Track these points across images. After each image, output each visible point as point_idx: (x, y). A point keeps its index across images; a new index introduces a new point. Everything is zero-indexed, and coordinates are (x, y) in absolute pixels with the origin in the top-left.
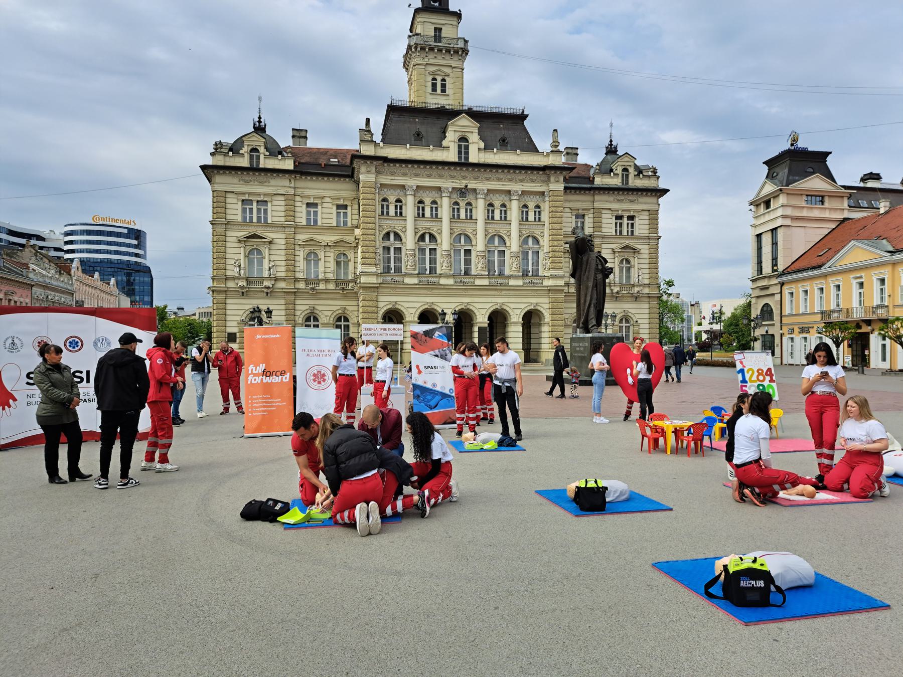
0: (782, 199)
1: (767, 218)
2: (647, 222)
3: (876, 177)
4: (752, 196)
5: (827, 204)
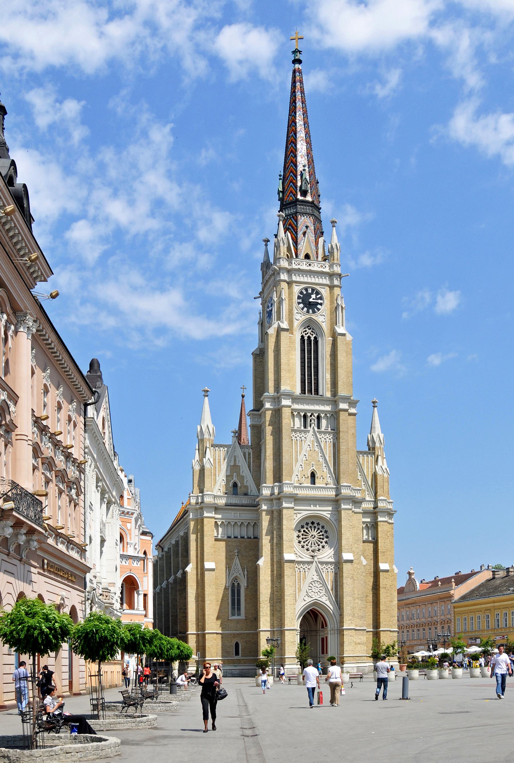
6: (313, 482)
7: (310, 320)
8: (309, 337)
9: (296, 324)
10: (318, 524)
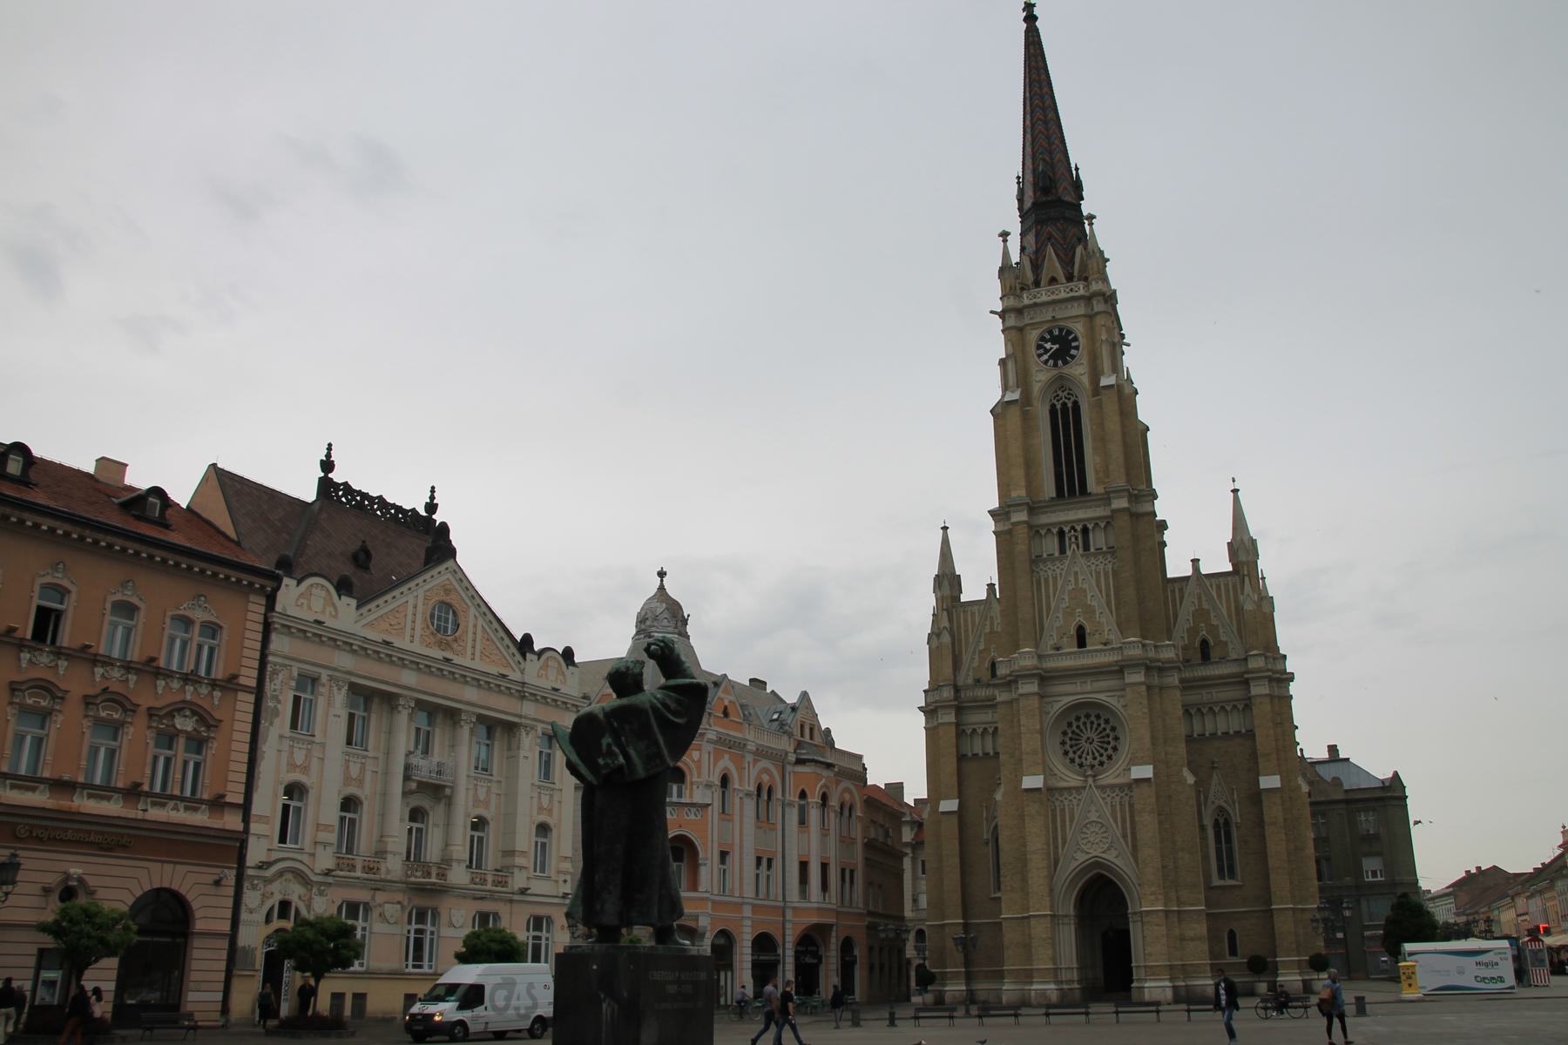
6: (1082, 642)
7: (1061, 377)
8: (1064, 404)
9: (1036, 388)
10: (1098, 717)
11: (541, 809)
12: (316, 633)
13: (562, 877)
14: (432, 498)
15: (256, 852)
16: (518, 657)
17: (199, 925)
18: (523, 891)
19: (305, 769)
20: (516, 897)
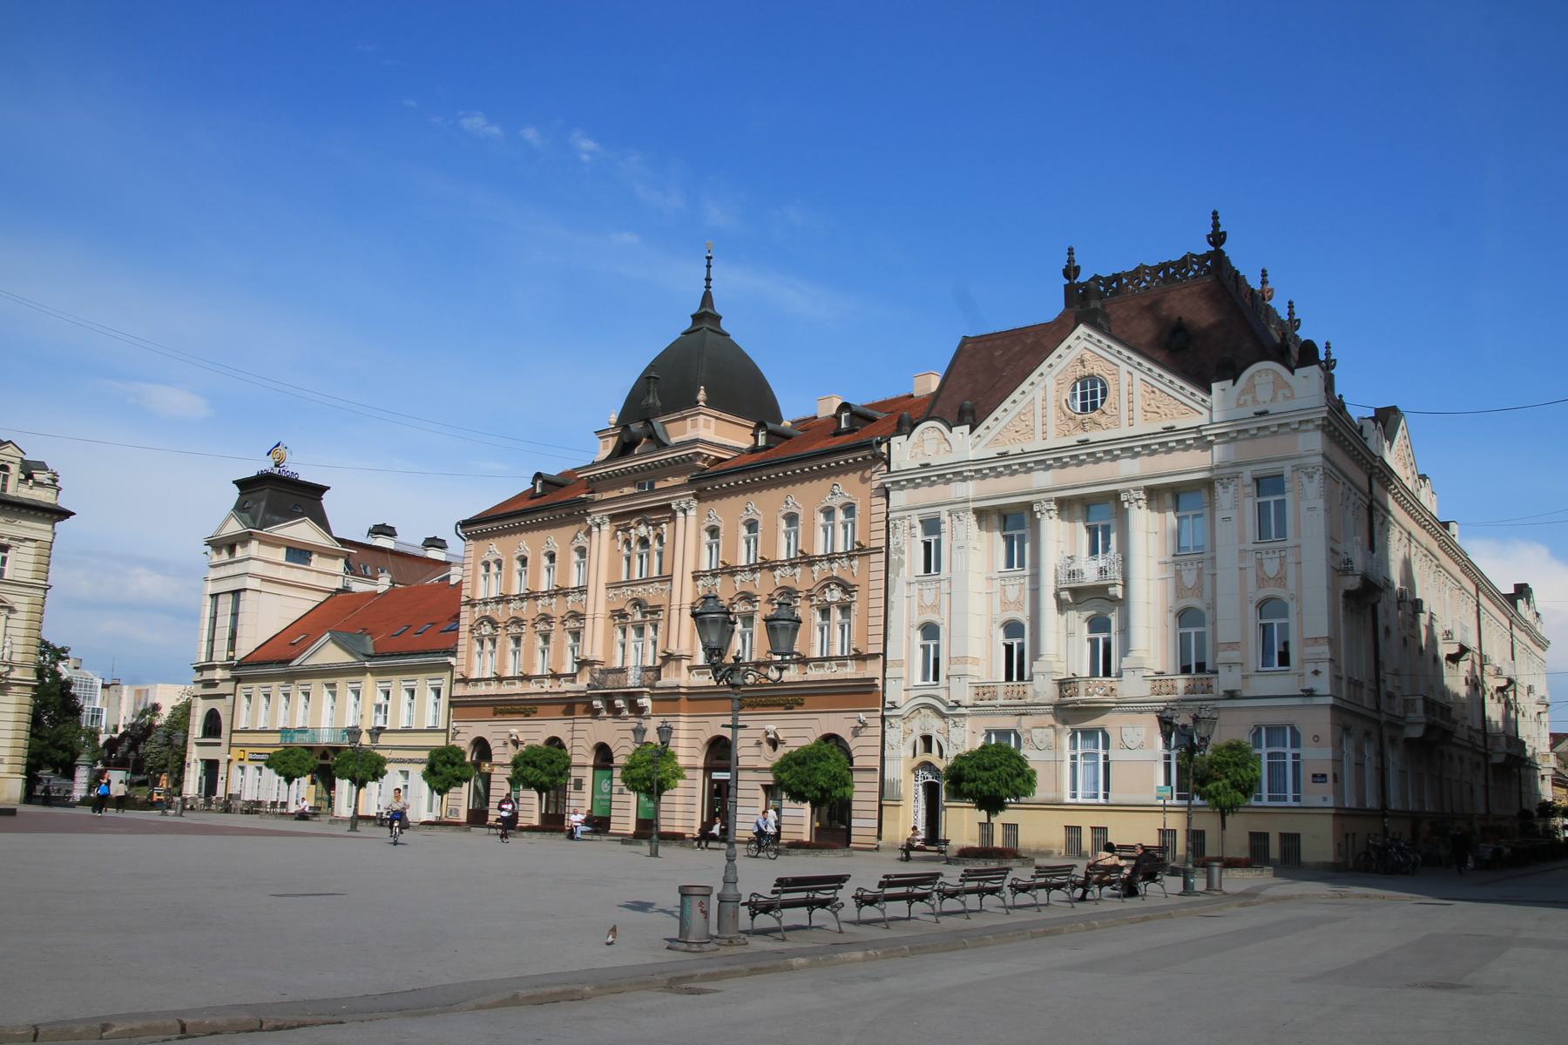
0: (254, 548)
1: (231, 570)
2: (32, 559)
3: (387, 531)
4: (210, 532)
5: (313, 565)
11: (1262, 581)
12: (928, 475)
13: (1311, 667)
14: (1216, 225)
15: (894, 693)
16: (1200, 395)
17: (857, 763)
18: (1231, 695)
19: (936, 607)
20: (1221, 704)
